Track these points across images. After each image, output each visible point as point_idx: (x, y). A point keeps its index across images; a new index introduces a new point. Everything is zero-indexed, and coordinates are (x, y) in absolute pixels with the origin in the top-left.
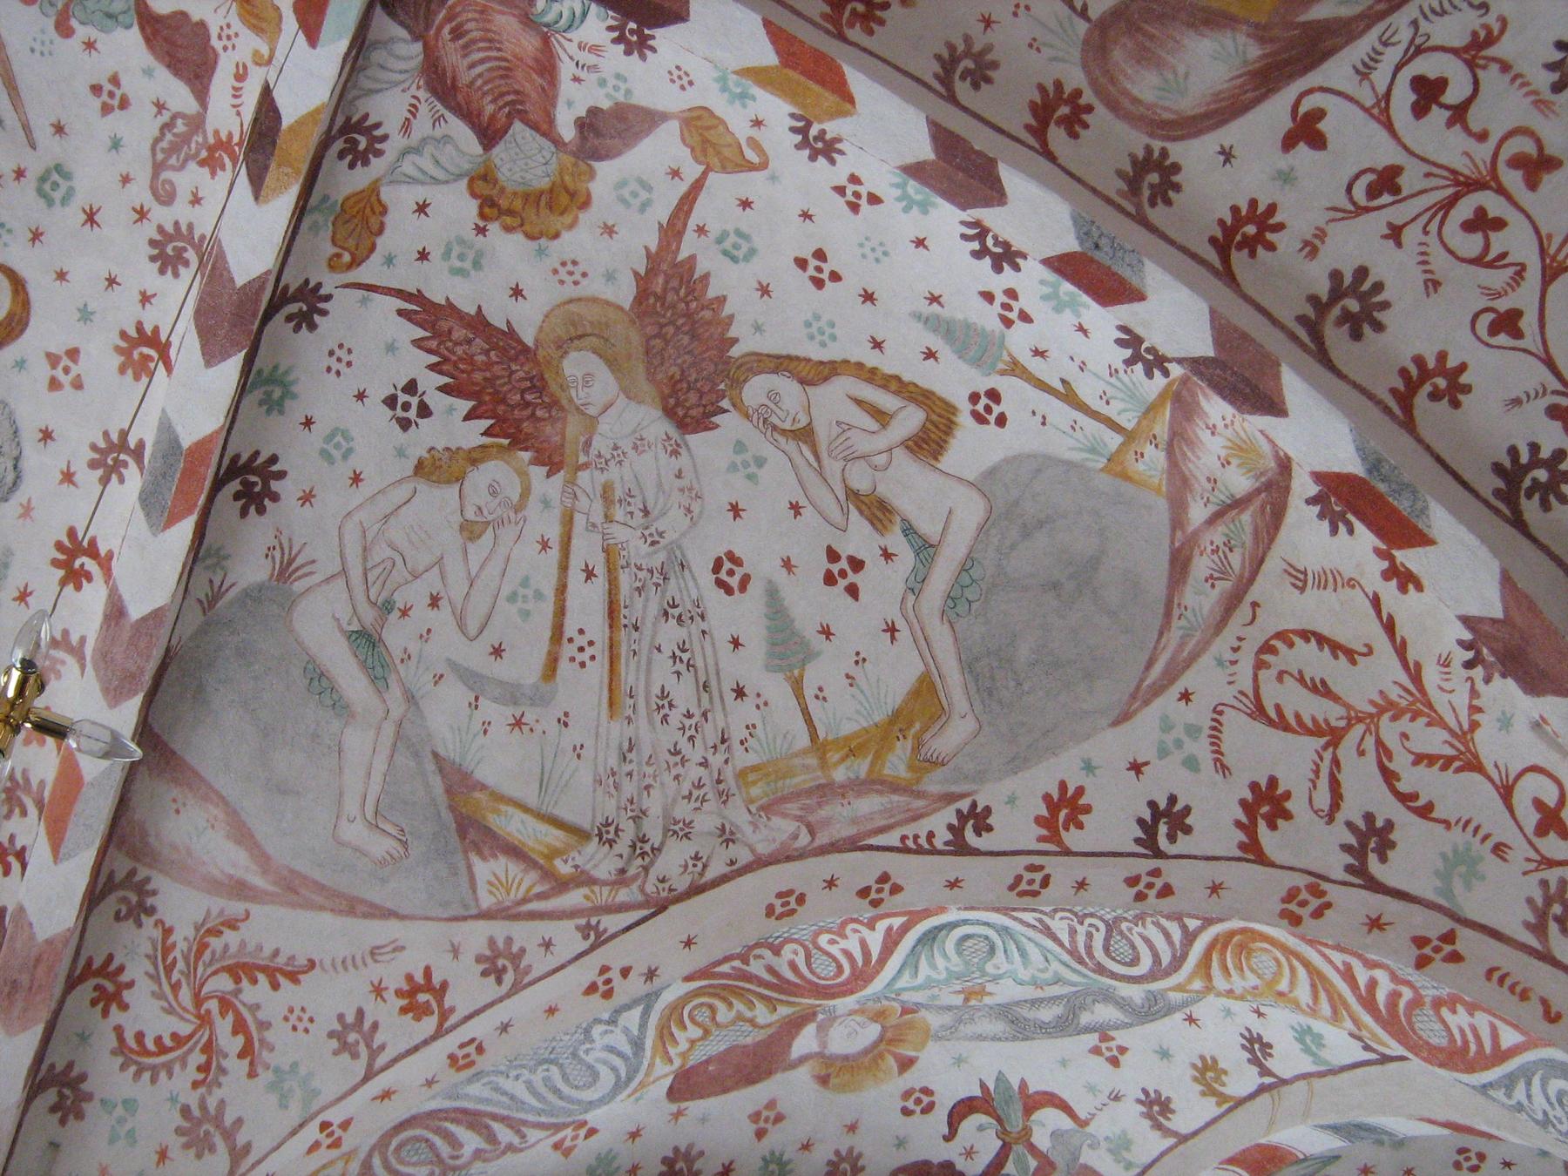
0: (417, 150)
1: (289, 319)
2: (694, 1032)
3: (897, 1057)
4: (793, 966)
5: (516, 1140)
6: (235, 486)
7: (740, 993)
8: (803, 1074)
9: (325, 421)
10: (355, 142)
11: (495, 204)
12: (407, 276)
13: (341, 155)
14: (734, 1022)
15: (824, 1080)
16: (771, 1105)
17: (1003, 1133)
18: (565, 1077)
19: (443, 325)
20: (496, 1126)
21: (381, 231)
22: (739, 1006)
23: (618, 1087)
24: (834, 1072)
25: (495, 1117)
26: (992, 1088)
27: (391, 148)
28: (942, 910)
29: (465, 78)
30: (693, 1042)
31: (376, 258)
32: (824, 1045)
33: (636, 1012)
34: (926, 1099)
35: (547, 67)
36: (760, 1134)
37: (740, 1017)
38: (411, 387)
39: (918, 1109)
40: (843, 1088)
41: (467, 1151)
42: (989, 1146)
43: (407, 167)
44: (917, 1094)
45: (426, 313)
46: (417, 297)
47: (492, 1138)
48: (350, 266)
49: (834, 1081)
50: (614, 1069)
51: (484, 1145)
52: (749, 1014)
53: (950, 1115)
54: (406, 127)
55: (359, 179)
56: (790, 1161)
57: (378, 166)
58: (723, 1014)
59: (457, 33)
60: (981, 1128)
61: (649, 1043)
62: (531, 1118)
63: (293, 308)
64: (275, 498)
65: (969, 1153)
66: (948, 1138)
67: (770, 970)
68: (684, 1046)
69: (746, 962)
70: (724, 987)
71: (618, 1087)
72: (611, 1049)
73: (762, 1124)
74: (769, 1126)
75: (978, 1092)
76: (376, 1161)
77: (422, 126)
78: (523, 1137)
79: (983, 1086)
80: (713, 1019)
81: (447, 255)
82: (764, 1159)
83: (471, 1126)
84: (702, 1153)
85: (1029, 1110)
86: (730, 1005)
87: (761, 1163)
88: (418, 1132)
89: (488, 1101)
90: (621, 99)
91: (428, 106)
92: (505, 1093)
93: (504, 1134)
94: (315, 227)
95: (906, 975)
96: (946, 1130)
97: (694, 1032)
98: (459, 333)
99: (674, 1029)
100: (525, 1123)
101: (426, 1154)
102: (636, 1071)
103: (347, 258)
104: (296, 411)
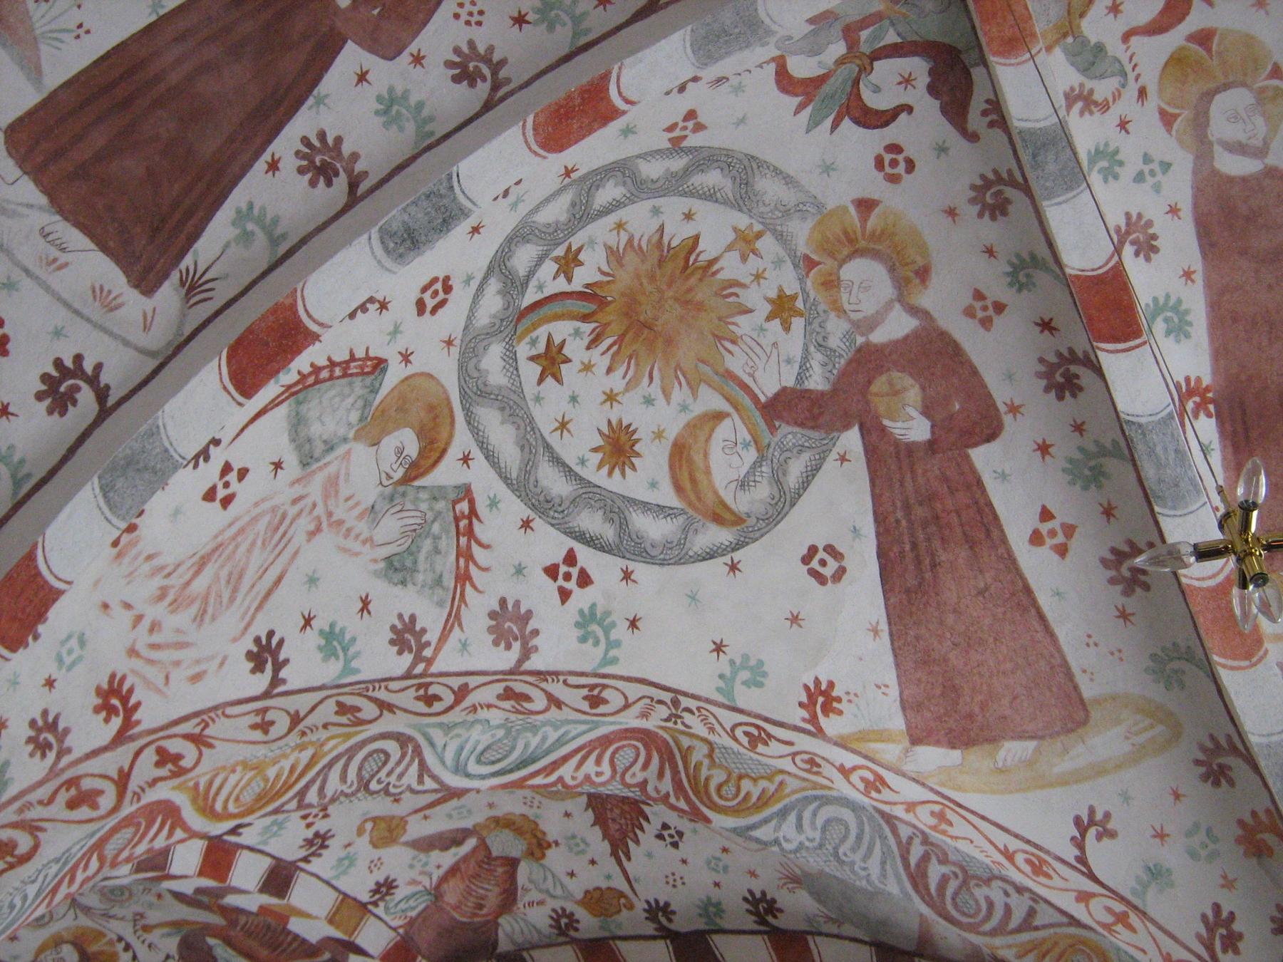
0: (547, 891)
1: (670, 920)
2: (746, 785)
3: (864, 220)
4: (646, 766)
5: (917, 841)
6: (770, 919)
7: (694, 780)
8: (927, 299)
9: (708, 877)
10: (566, 924)
11: (539, 846)
12: (610, 865)
13: (576, 930)
14: (721, 766)
15: (923, 274)
16: (969, 312)
17: (866, 69)
18: (844, 839)
19: (617, 835)
20: (913, 861)
21: (598, 889)
22: (704, 773)
23: (826, 801)
24: (910, 273)
25: (906, 865)
26: (828, 122)
27: (557, 904)
28: (493, 788)
29: (497, 890)
30: (755, 780)
31: (613, 884)
32: (888, 306)
33: (757, 833)
34: (888, 158)
35: (453, 871)
36: (999, 308)
37: (713, 764)
38: (660, 837)
39: (900, 158)
40: (923, 248)
41: (945, 869)
42: (886, 70)
43: (559, 892)
44: (888, 170)
45: (619, 848)
46: (614, 853)
47: (925, 858)
48: (625, 897)
49: (920, 262)
50: (814, 814)
51: (934, 860)
52: (706, 762)
53: (887, 124)
54: (541, 903)
55: (581, 913)
56: (1010, 263)
57: (570, 907)
58: (718, 776)
59: (480, 907)
60: (877, 89)
61: (777, 807)
62: (892, 841)
63: (663, 920)
64: (764, 893)
65: (907, 81)
66: (909, 109)
67: (661, 775)
68: (763, 784)
69: (667, 795)
70: (697, 793)
71: (826, 801)
72: (799, 827)
73: (991, 312)
74: (989, 303)
75: (847, 123)
76: (987, 927)
77: (535, 895)
78: (910, 838)
79: (835, 125)
80: (727, 781)
81: (583, 852)
82: (1019, 290)
83: (924, 875)
84: (1041, 360)
85: (820, 81)
86: (707, 779)
87: (1025, 292)
88: (950, 907)
89: (897, 876)
90: (422, 856)
91: (523, 899)
92: (883, 869)
93: (917, 851)
94: (619, 926)
95: (572, 734)
96: (903, 116)
97: (746, 785)
98: (613, 827)
99: (754, 799)
100: (899, 843)
101: (964, 896)
102: (806, 798)
103: (623, 901)
104: (715, 894)
